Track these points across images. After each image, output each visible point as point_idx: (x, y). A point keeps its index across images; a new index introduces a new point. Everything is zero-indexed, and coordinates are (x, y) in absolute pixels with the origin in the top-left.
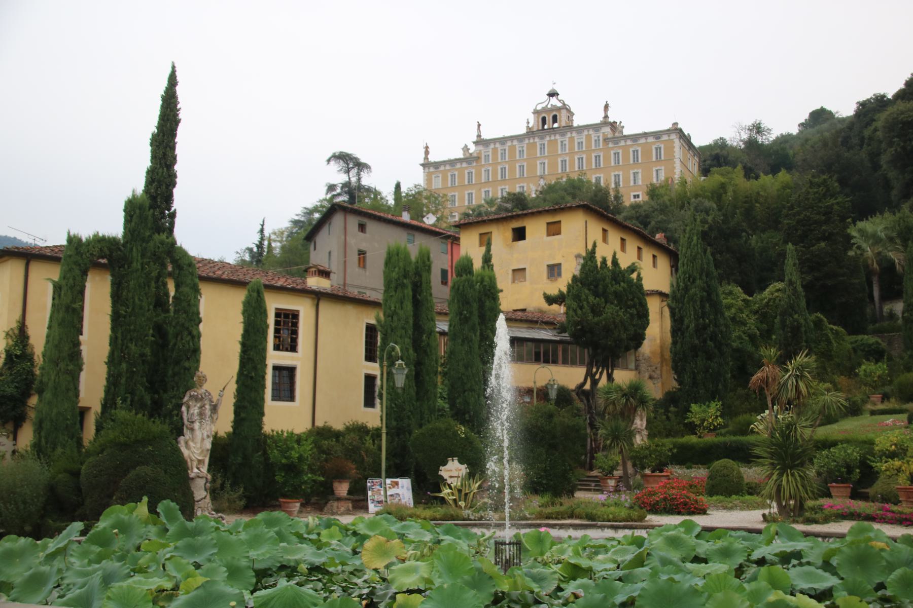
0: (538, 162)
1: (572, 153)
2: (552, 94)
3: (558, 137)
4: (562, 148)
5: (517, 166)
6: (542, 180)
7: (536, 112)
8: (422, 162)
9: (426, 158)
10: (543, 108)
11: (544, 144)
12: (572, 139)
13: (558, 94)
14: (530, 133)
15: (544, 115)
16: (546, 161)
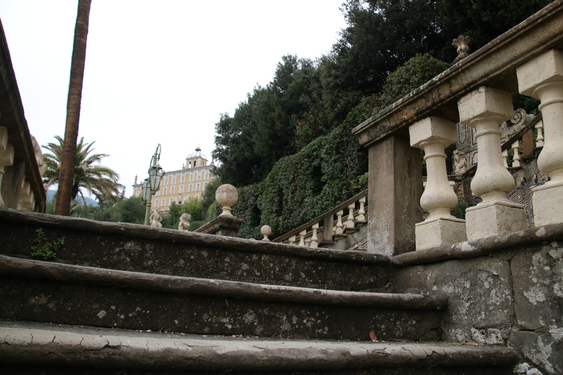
0: (180, 186)
1: (195, 181)
2: (198, 150)
3: (190, 173)
4: (191, 179)
5: (171, 187)
6: (180, 196)
7: (188, 159)
8: (133, 184)
9: (136, 182)
10: (191, 157)
11: (184, 176)
12: (196, 173)
13: (200, 150)
14: (185, 170)
15: (190, 161)
16: (184, 186)
